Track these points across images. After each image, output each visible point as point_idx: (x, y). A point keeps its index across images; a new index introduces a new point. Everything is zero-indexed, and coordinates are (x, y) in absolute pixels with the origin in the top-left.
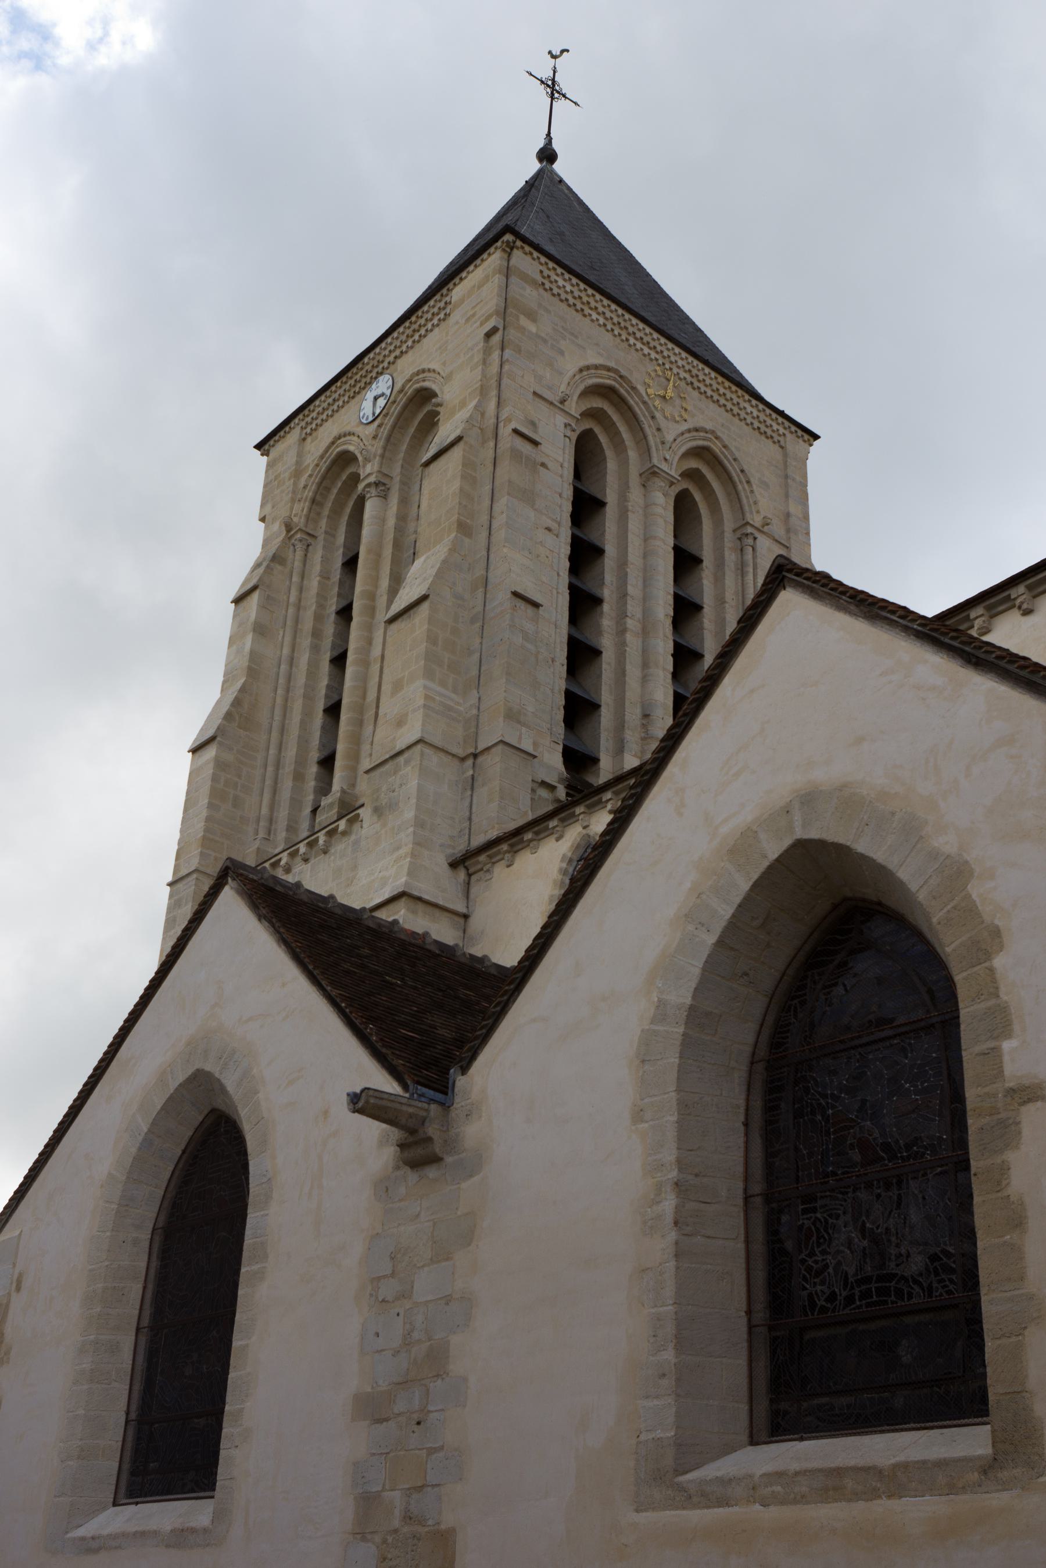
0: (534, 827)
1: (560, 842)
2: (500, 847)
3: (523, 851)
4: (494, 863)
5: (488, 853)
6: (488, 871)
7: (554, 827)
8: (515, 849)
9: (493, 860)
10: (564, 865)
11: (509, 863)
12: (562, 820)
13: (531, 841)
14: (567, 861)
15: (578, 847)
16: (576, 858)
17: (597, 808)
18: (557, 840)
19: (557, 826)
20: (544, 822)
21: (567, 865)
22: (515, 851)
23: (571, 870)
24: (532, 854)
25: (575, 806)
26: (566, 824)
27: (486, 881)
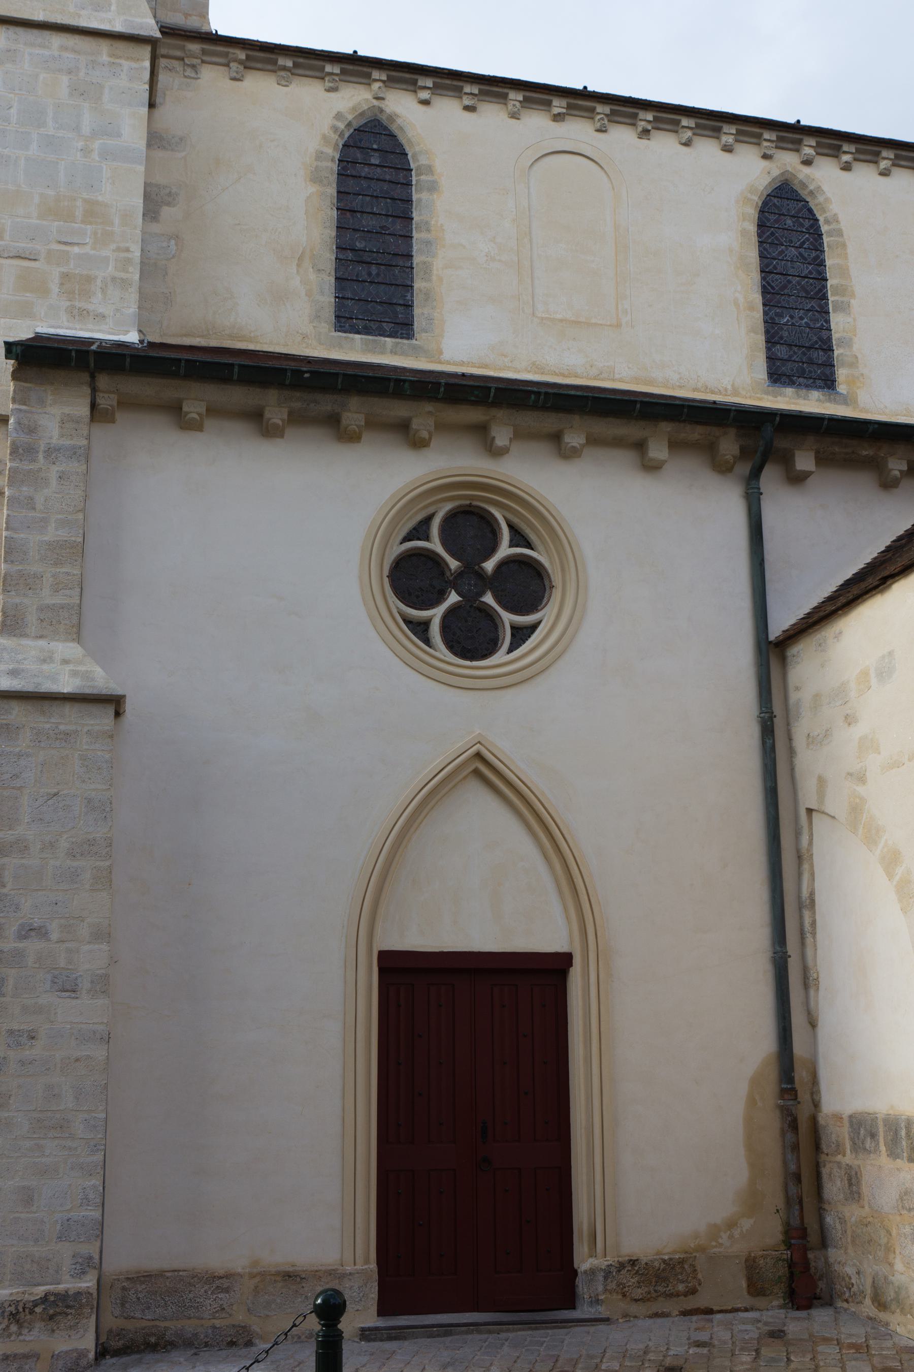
0: (301, 57)
1: (332, 95)
2: (231, 50)
3: (262, 72)
4: (203, 62)
5: (205, 46)
6: (193, 67)
7: (332, 74)
8: (249, 64)
9: (205, 58)
10: (341, 126)
11: (238, 76)
12: (343, 72)
13: (284, 68)
14: (346, 123)
15: (362, 114)
16: (356, 125)
17: (397, 86)
18: (329, 90)
19: (336, 75)
20: (369, 66)
21: (345, 127)
22: (248, 65)
23: (347, 135)
24: (278, 84)
25: (376, 68)
26: (343, 77)
27: (185, 77)
